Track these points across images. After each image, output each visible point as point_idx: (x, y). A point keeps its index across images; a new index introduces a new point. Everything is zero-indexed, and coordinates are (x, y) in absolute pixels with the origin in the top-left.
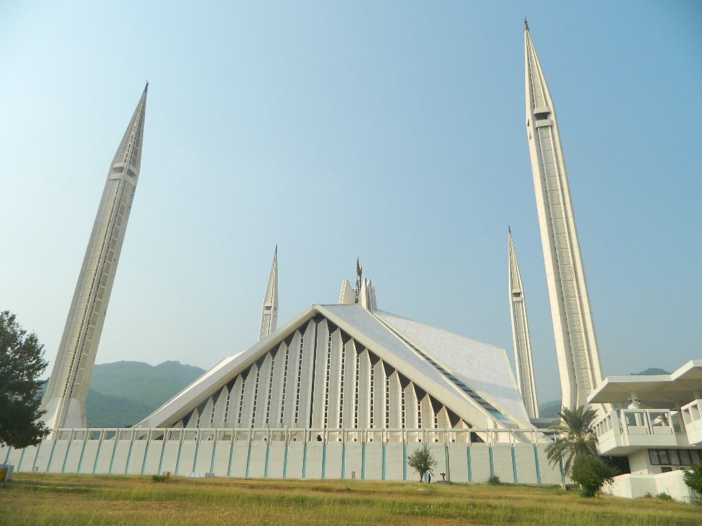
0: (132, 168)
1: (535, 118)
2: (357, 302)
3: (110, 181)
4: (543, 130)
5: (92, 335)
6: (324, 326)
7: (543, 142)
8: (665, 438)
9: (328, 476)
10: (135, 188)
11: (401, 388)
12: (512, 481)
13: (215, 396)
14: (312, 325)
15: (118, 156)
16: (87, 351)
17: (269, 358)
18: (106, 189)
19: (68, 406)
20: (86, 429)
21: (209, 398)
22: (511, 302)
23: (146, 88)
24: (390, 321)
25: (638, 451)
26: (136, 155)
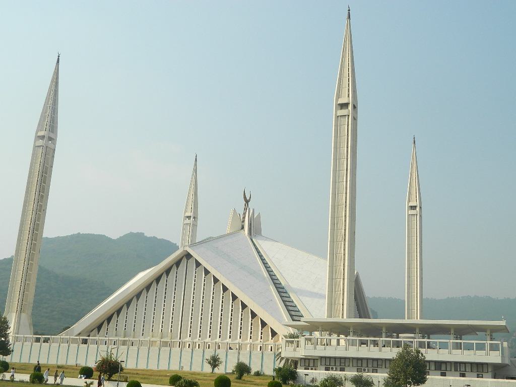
0: (52, 135)
1: (338, 106)
2: (243, 228)
3: (36, 147)
4: (342, 119)
5: (32, 268)
6: (192, 263)
7: (340, 130)
10: (55, 150)
13: (119, 312)
14: (185, 260)
16: (29, 280)
18: (33, 154)
19: (20, 318)
20: (31, 336)
23: (58, 59)
26: (53, 123)
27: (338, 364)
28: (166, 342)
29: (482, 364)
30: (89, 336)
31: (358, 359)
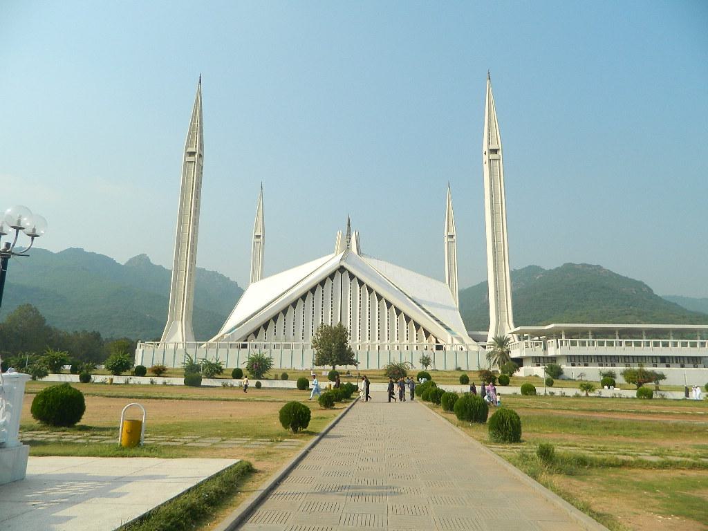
0: (202, 153)
3: (185, 162)
6: (346, 275)
8: (539, 352)
9: (371, 367)
10: (202, 167)
11: (396, 316)
12: (466, 369)
14: (338, 275)
15: (189, 143)
17: (310, 295)
18: (184, 169)
21: (269, 321)
22: (446, 238)
23: (200, 80)
24: (372, 263)
25: (527, 358)
27: (582, 360)
28: (290, 345)
29: (696, 358)
30: (246, 340)
31: (598, 356)
